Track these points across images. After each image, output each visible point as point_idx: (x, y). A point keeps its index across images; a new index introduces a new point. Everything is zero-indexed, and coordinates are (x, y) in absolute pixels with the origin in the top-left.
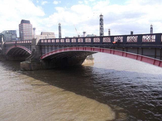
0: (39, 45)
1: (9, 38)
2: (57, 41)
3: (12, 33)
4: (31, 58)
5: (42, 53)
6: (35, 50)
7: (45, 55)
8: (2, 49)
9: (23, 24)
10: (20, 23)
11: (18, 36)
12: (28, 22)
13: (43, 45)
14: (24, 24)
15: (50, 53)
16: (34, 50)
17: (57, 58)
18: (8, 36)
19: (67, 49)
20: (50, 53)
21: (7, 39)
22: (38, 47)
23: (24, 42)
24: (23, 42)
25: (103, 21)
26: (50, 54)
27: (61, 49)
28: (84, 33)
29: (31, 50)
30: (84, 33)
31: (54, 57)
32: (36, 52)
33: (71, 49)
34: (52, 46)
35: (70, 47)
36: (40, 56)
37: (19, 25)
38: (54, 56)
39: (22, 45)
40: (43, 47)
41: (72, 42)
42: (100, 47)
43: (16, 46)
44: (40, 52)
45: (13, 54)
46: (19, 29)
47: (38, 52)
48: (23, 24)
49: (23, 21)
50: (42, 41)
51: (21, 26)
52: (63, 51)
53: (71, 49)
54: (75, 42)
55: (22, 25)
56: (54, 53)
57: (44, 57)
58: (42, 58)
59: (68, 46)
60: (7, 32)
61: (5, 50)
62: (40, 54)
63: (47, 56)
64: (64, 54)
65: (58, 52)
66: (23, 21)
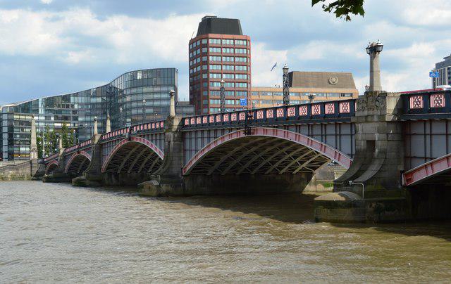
2: (280, 113)
3: (165, 76)
5: (408, 159)
7: (431, 164)
8: (167, 152)
9: (208, 38)
10: (192, 31)
11: (184, 94)
12: (231, 27)
14: (214, 39)
16: (371, 144)
21: (134, 112)
23: (212, 120)
24: (205, 120)
29: (338, 146)
32: (383, 152)
36: (402, 172)
37: (192, 42)
40: (419, 129)
41: (432, 105)
46: (191, 59)
47: (393, 154)
48: (211, 35)
49: (209, 26)
50: (413, 103)
51: (198, 48)
54: (421, 106)
55: (204, 42)
57: (420, 176)
58: (409, 180)
60: (139, 76)
61: (182, 154)
66: (209, 26)
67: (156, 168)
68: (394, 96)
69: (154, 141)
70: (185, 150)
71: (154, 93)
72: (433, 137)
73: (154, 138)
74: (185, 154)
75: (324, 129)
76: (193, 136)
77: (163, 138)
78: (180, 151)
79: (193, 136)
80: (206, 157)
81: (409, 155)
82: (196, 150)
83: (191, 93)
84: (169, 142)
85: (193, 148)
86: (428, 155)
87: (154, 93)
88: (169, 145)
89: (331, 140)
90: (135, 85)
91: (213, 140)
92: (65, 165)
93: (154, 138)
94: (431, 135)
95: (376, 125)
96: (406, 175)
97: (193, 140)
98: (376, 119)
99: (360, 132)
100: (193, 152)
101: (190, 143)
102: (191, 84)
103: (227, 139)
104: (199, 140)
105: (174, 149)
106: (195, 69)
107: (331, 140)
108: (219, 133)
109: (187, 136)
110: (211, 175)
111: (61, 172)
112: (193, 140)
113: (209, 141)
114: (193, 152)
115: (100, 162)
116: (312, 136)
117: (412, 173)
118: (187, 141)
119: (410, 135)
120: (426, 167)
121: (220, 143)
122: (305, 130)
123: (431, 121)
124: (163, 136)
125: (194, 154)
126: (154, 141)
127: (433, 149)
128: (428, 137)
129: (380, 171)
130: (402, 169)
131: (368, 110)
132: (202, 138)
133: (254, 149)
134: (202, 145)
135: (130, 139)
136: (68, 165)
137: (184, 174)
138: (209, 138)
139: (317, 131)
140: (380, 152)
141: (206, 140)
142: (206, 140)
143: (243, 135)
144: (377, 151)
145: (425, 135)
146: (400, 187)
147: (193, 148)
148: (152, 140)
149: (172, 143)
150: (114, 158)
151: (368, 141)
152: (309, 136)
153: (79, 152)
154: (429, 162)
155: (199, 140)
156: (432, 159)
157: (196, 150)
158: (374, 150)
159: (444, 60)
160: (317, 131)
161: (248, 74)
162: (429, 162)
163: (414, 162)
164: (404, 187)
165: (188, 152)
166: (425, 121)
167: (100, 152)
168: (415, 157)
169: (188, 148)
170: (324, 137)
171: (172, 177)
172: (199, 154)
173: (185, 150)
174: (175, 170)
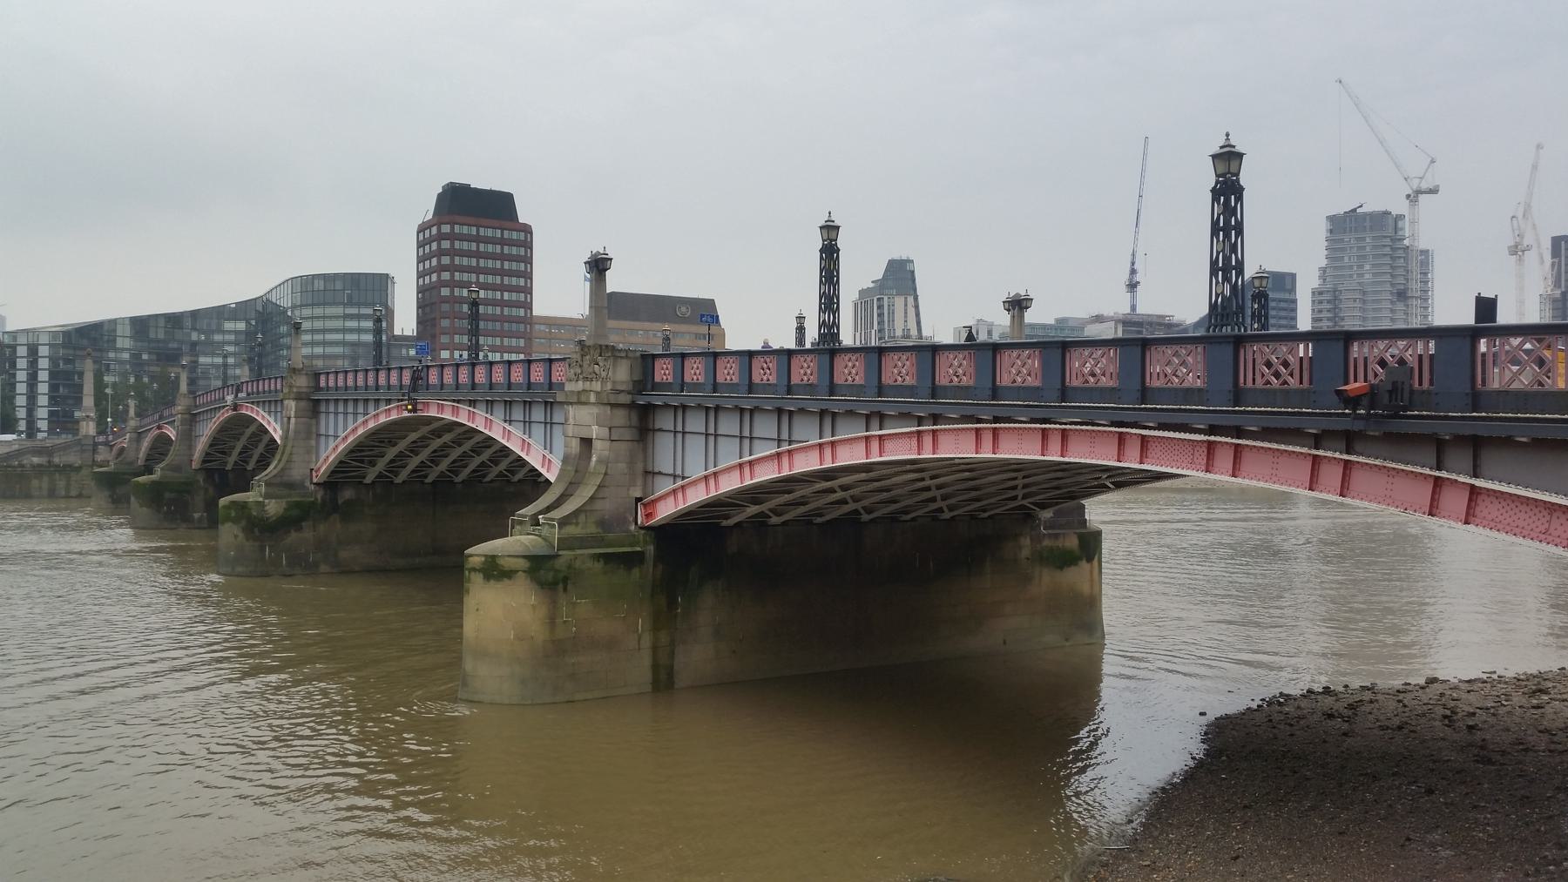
0: (632, 406)
1: (324, 343)
4: (558, 514)
6: (597, 445)
7: (683, 487)
8: (285, 437)
13: (666, 406)
15: (728, 470)
17: (775, 520)
18: (318, 324)
19: (888, 445)
20: (728, 470)
22: (621, 417)
25: (1240, 199)
26: (730, 484)
27: (833, 444)
28: (1018, 305)
29: (548, 445)
30: (1018, 305)
31: (753, 510)
33: (928, 440)
34: (752, 412)
35: (920, 421)
36: (638, 500)
38: (756, 502)
39: (472, 403)
40: (665, 421)
42: (1212, 430)
43: (414, 410)
44: (639, 467)
45: (380, 475)
52: (851, 456)
53: (928, 440)
56: (766, 474)
57: (666, 510)
58: (649, 516)
59: (905, 416)
62: (639, 482)
63: (697, 496)
64: (844, 488)
65: (807, 463)
67: (263, 463)
68: (627, 357)
69: (273, 414)
70: (319, 435)
71: (324, 317)
72: (720, 439)
73: (273, 409)
74: (318, 443)
75: (508, 407)
76: (332, 409)
77: (279, 410)
78: (308, 437)
79: (332, 409)
80: (352, 451)
81: (651, 469)
82: (336, 437)
83: (421, 322)
84: (289, 418)
85: (331, 432)
86: (679, 472)
87: (324, 317)
88: (289, 422)
89: (538, 430)
90: (310, 302)
91: (361, 419)
92: (138, 450)
93: (273, 409)
94: (684, 433)
95: (595, 410)
96: (645, 505)
97: (332, 416)
98: (593, 398)
99: (571, 421)
100: (331, 439)
101: (327, 423)
102: (421, 306)
103: (383, 419)
104: (341, 417)
105: (296, 432)
106: (427, 278)
107: (538, 430)
108: (371, 406)
109: (323, 408)
110: (373, 482)
111: (131, 463)
112: (332, 416)
113: (355, 420)
114: (331, 439)
115: (191, 447)
116: (511, 422)
117: (654, 502)
118: (323, 417)
119: (654, 430)
120: (674, 491)
121: (371, 425)
122: (499, 411)
123: (717, 409)
124: (279, 405)
125: (332, 445)
126: (273, 414)
127: (687, 459)
128: (712, 439)
129: (592, 498)
130: (639, 495)
131: (586, 379)
132: (346, 414)
133: (447, 438)
134: (345, 429)
135: (235, 407)
136: (143, 449)
137: (315, 480)
138: (355, 414)
139: (518, 414)
140: (599, 461)
141: (350, 418)
142: (350, 418)
143: (406, 414)
144: (594, 459)
145: (675, 432)
146: (633, 527)
147: (331, 432)
148: (270, 412)
149: (293, 420)
150: (215, 442)
151: (582, 439)
152: (505, 421)
153: (159, 427)
154: (680, 483)
155: (341, 417)
156: (683, 478)
157: (336, 437)
158: (590, 457)
159: (872, 285)
160: (518, 414)
161: (528, 291)
162: (680, 483)
163: (659, 480)
164: (641, 528)
165: (323, 439)
166: (707, 409)
167: (191, 430)
168: (660, 473)
169: (323, 431)
170: (527, 424)
171: (291, 486)
172: (340, 443)
173: (319, 435)
174: (297, 473)
